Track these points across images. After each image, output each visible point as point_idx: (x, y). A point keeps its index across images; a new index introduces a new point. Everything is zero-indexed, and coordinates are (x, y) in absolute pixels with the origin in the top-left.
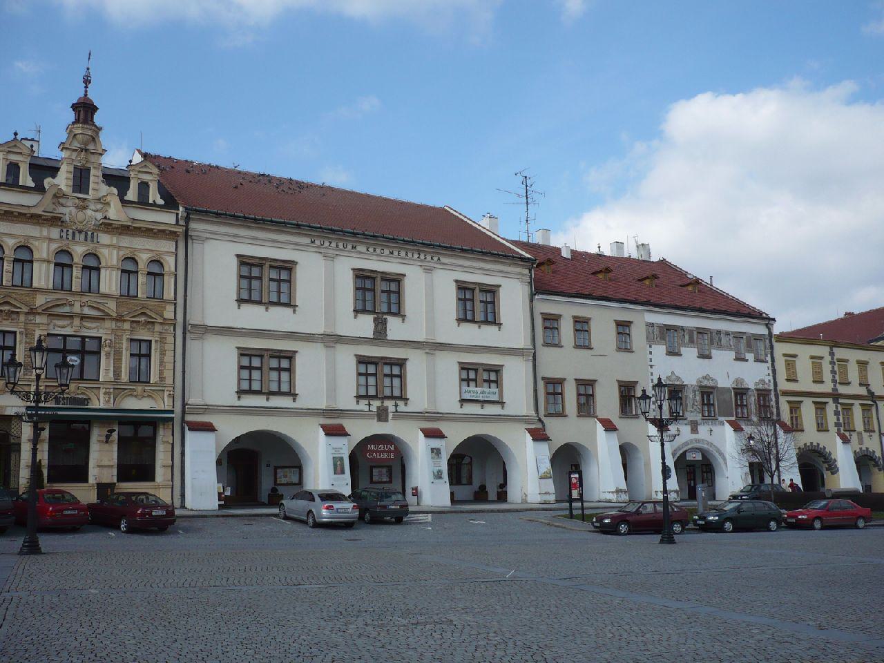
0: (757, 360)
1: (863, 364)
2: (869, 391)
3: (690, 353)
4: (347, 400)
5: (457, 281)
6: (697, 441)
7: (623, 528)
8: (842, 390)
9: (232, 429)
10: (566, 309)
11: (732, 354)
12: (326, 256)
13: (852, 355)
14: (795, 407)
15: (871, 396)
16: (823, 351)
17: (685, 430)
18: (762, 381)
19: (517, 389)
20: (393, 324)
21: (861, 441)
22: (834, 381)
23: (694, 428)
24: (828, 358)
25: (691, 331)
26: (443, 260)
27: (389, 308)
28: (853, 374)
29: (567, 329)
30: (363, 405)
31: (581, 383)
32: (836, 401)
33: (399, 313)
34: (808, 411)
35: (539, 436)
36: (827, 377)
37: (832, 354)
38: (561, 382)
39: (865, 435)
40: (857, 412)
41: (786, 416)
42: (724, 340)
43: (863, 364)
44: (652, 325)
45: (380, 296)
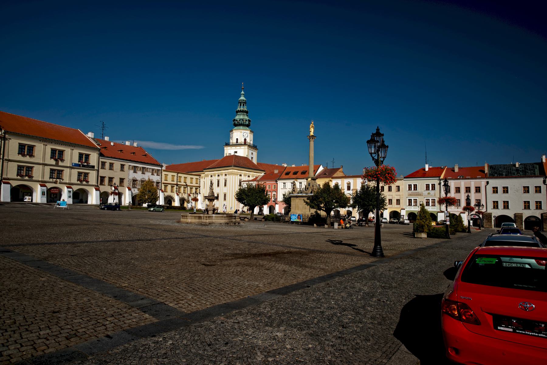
0: (157, 175)
3: (139, 173)
4: (47, 178)
8: (179, 183)
9: (15, 183)
10: (108, 161)
14: (166, 186)
15: (187, 185)
16: (175, 174)
20: (60, 163)
25: (140, 168)
28: (182, 180)
29: (107, 166)
30: (51, 180)
31: (109, 178)
34: (169, 187)
35: (97, 189)
36: (175, 180)
38: (104, 177)
40: (182, 189)
41: (163, 189)
43: (185, 178)
45: (57, 155)
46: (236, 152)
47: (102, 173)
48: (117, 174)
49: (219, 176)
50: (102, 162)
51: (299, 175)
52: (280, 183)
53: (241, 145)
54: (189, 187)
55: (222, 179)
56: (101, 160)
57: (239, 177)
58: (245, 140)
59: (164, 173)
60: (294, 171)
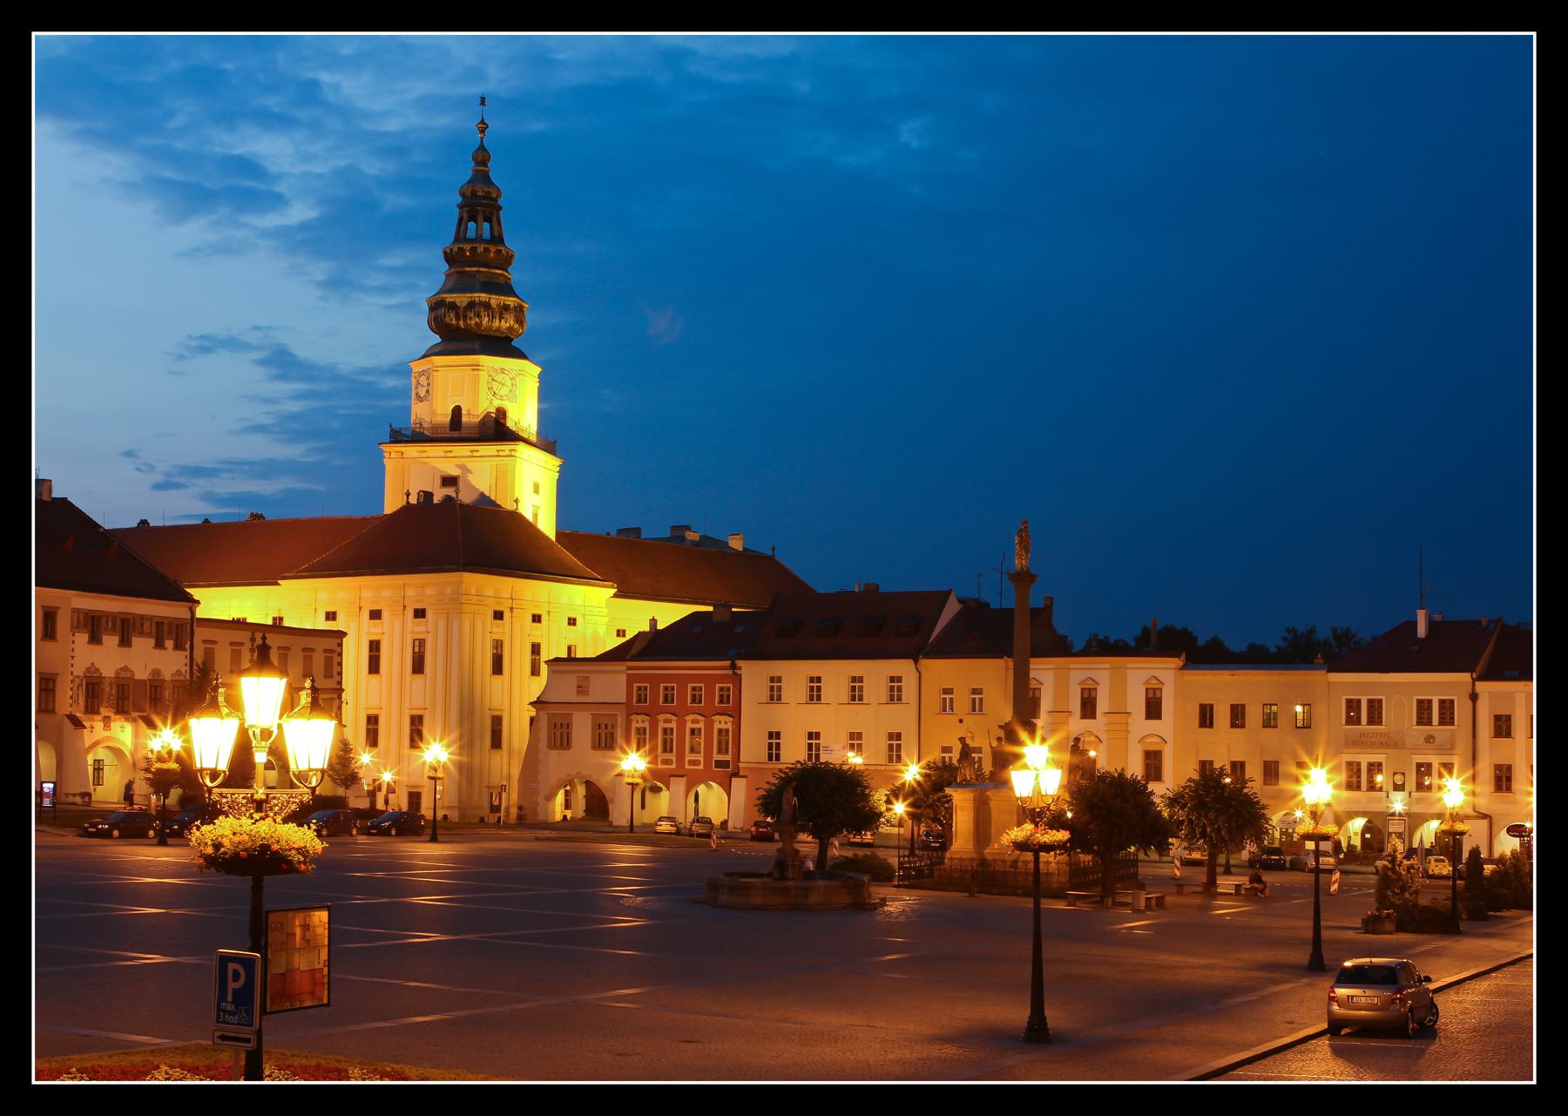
3: (111, 641)
6: (109, 739)
7: (116, 833)
11: (152, 642)
17: (99, 725)
18: (178, 672)
23: (107, 720)
42: (147, 625)
46: (449, 481)
52: (755, 675)
59: (201, 634)
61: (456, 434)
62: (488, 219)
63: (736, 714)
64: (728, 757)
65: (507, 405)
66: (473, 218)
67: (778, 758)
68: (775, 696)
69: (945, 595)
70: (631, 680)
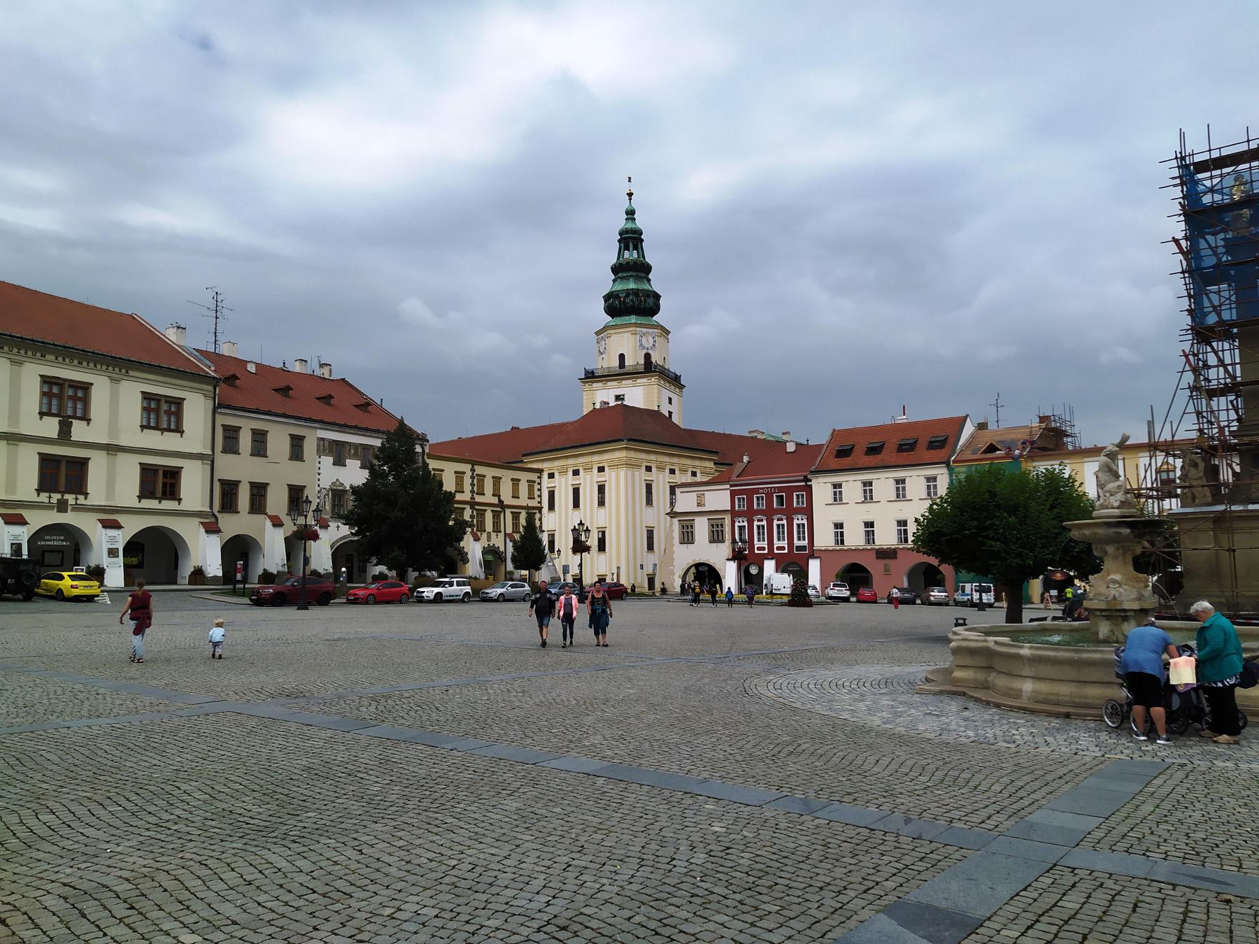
1: (497, 480)
2: (500, 501)
5: (143, 393)
8: (478, 499)
10: (247, 426)
12: (12, 361)
13: (489, 473)
16: (466, 468)
19: (194, 489)
21: (489, 539)
22: (472, 492)
24: (469, 474)
26: (131, 373)
27: (75, 411)
28: (488, 486)
29: (245, 440)
30: (44, 497)
32: (472, 508)
33: (86, 418)
35: (212, 529)
36: (467, 488)
37: (473, 470)
39: (493, 535)
40: (489, 517)
43: (497, 480)
44: (323, 439)
46: (618, 398)
47: (229, 467)
48: (278, 472)
49: (576, 473)
50: (226, 428)
51: (888, 455)
53: (633, 374)
54: (508, 512)
55: (588, 483)
56: (221, 420)
57: (641, 475)
58: (647, 356)
60: (866, 445)
61: (622, 371)
62: (635, 248)
63: (809, 512)
64: (805, 543)
65: (650, 352)
66: (627, 248)
67: (842, 543)
68: (838, 498)
69: (964, 419)
70: (733, 494)
